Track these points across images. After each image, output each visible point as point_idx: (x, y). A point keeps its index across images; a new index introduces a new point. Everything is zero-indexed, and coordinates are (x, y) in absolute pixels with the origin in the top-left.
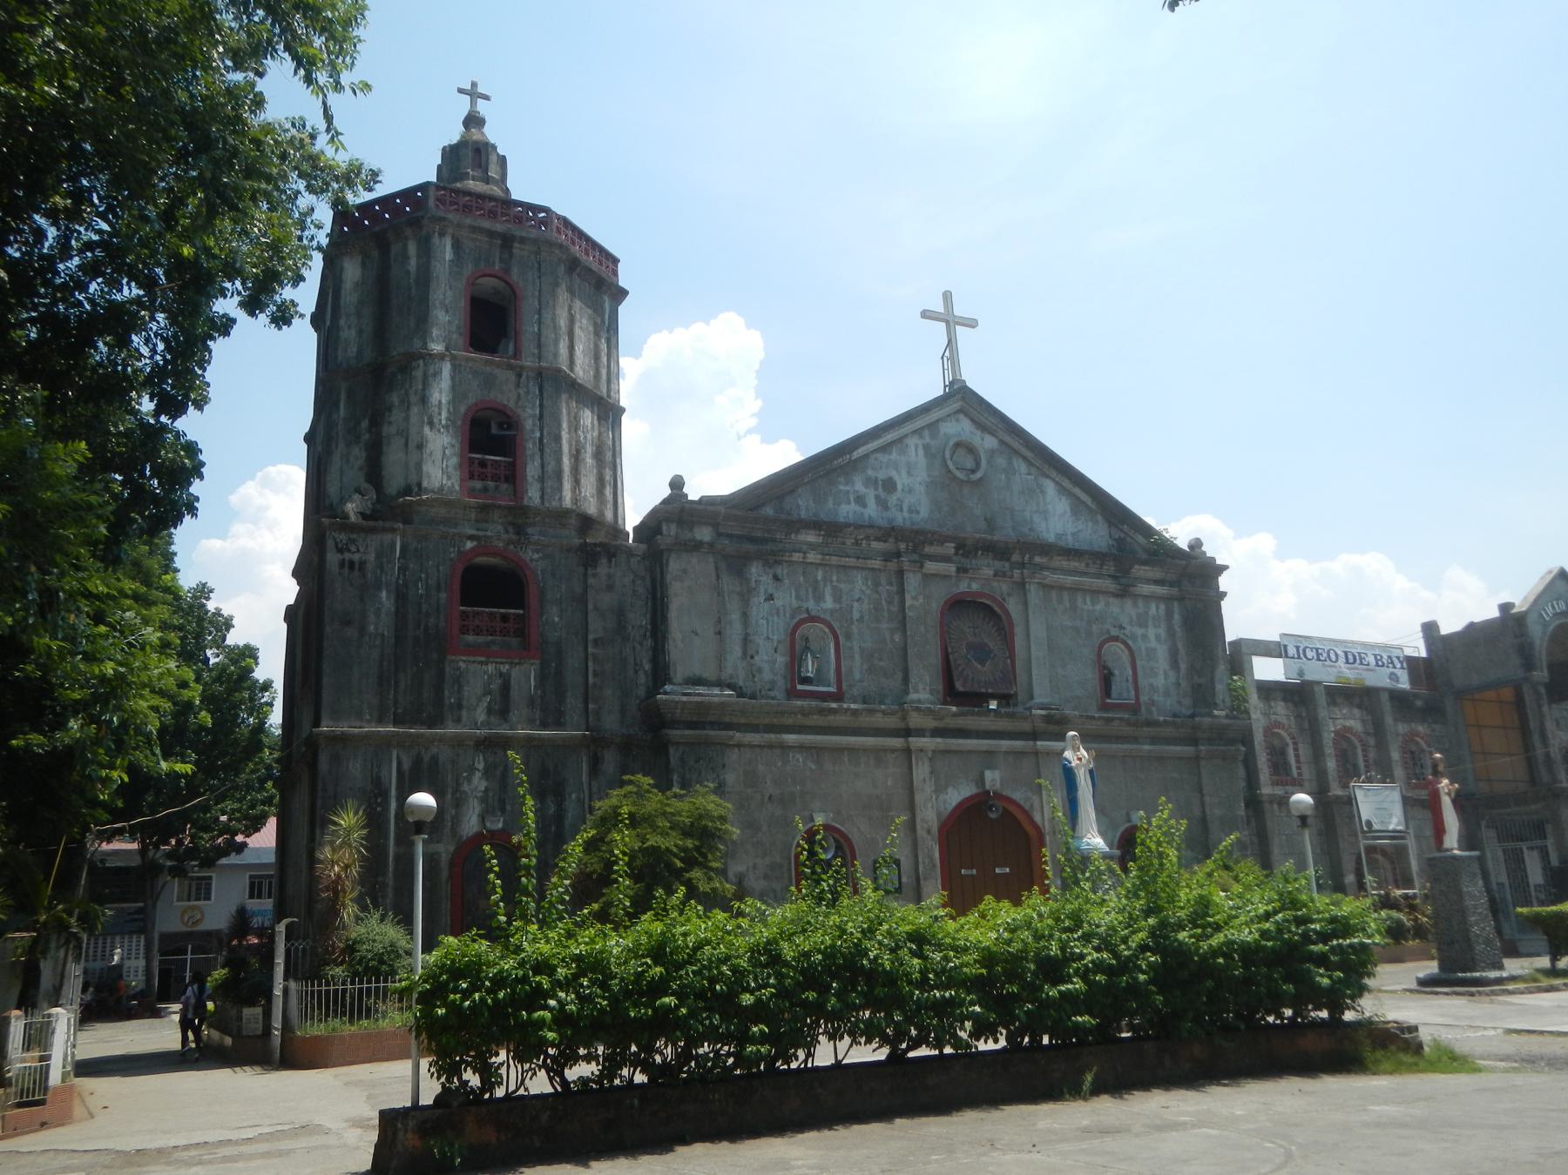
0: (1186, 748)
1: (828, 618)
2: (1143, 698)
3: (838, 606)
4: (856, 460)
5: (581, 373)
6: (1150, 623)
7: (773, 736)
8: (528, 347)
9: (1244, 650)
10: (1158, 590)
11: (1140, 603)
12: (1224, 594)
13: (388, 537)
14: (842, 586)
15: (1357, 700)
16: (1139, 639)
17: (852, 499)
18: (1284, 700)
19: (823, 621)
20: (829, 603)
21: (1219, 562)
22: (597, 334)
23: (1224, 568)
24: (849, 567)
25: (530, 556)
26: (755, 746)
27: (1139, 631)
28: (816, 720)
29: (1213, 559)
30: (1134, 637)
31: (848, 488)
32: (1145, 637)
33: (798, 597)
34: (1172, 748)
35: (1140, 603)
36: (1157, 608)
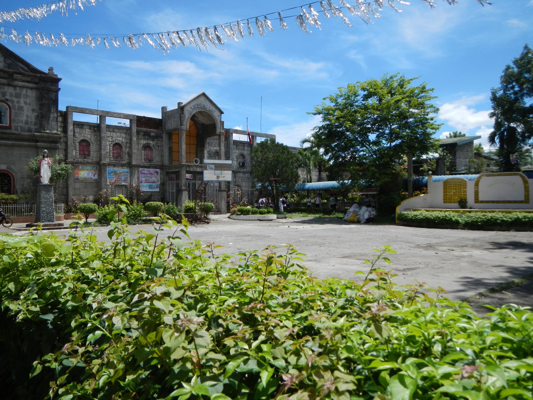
0: (32, 143)
2: (12, 125)
6: (22, 97)
9: (69, 110)
10: (27, 84)
11: (18, 89)
12: (59, 89)
15: (125, 131)
16: (15, 102)
18: (90, 129)
21: (59, 77)
23: (60, 80)
27: (15, 100)
29: (57, 75)
30: (12, 102)
32: (18, 102)
34: (25, 143)
35: (18, 89)
36: (27, 92)
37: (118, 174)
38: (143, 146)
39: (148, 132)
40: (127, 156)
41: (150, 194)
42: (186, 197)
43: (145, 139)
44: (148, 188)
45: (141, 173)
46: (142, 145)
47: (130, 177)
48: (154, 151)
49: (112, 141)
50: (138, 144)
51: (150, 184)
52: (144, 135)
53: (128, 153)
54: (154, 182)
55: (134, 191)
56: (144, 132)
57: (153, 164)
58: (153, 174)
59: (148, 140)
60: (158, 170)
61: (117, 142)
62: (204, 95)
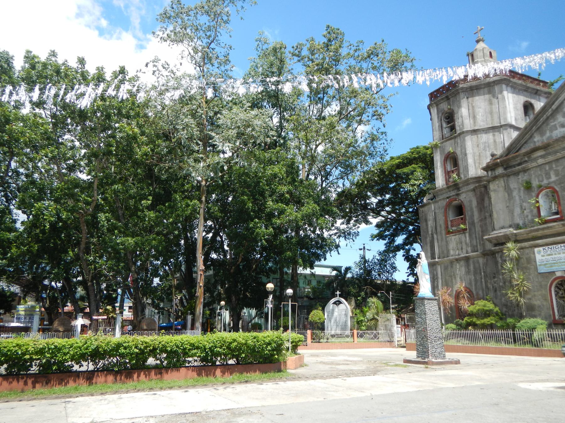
1: (552, 185)
3: (557, 178)
4: (557, 108)
5: (482, 123)
7: (532, 242)
8: (457, 128)
13: (430, 206)
14: (558, 168)
17: (558, 126)
19: (550, 188)
20: (553, 178)
22: (491, 103)
24: (561, 158)
25: (463, 197)
26: (528, 248)
28: (547, 232)
31: (555, 123)
33: (539, 181)
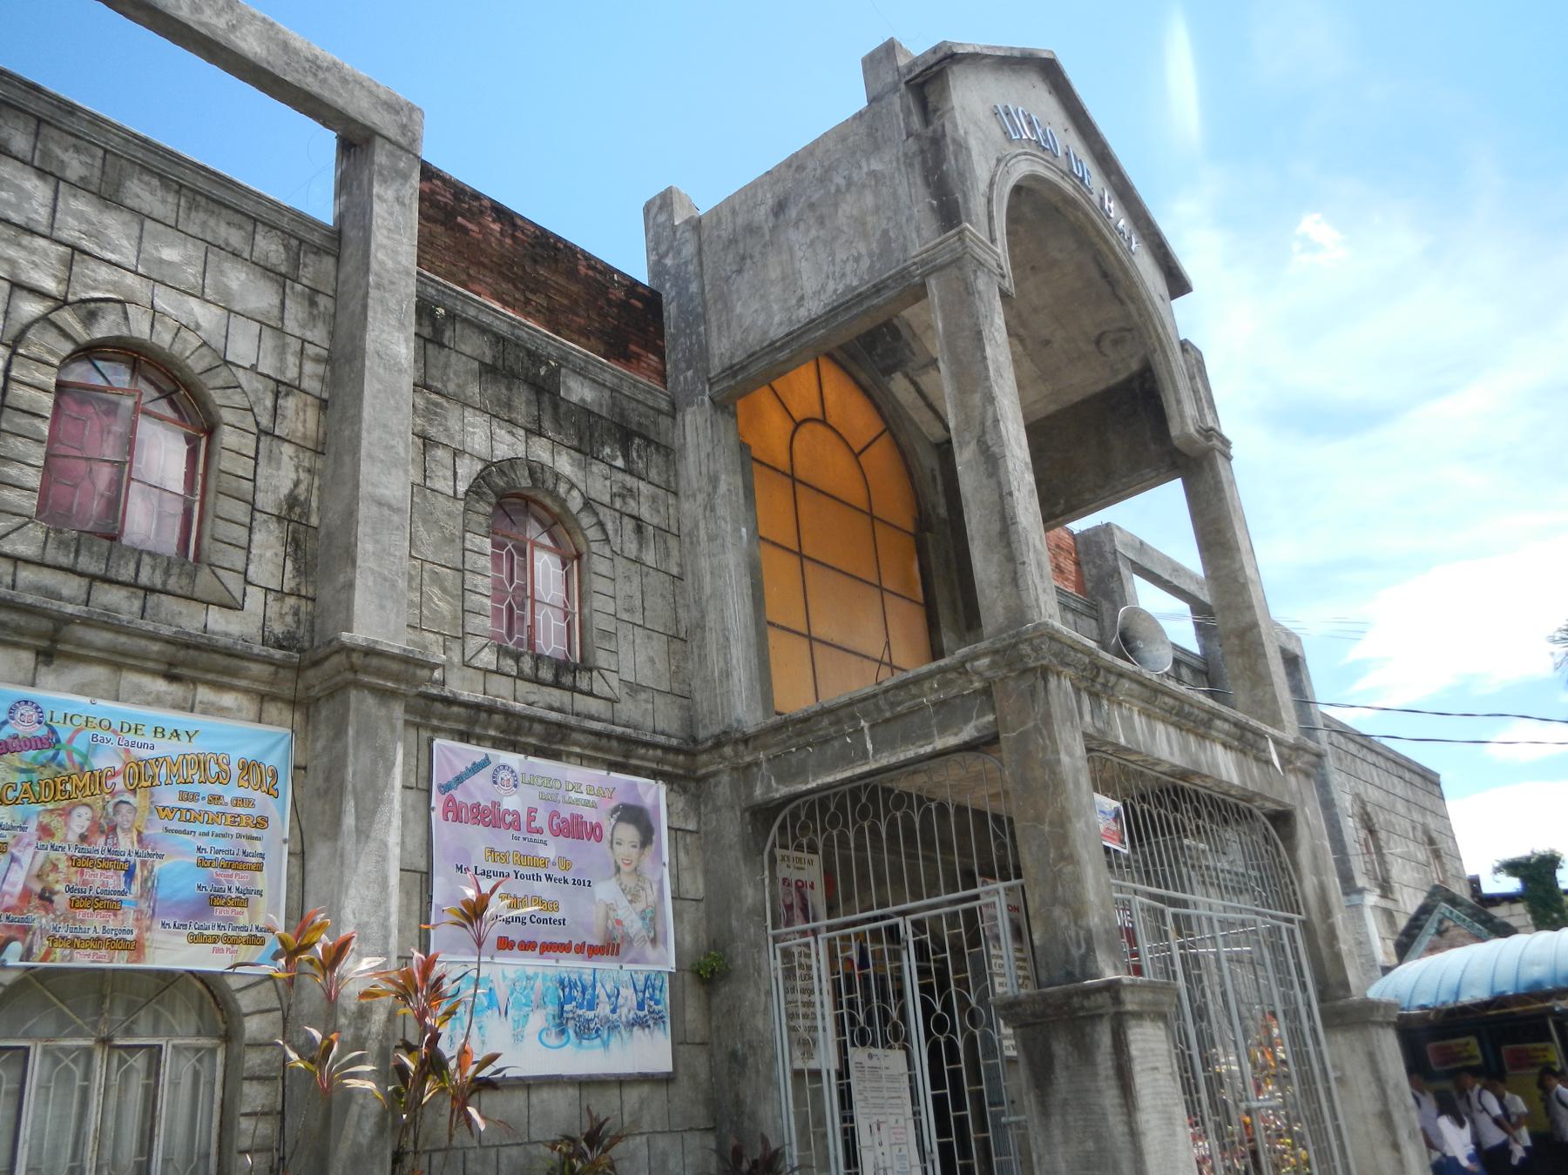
37: (99, 779)
38: (483, 478)
39: (535, 357)
40: (268, 544)
41: (560, 1109)
42: (1170, 1121)
43: (500, 414)
44: (538, 1020)
45: (455, 812)
46: (468, 470)
47: (300, 856)
48: (601, 566)
49: (62, 303)
50: (427, 442)
51: (571, 965)
52: (489, 371)
53: (293, 512)
54: (609, 948)
55: (364, 1082)
56: (499, 339)
57: (593, 705)
58: (595, 832)
59: (535, 431)
60: (653, 794)
61: (140, 327)
62: (1049, 71)
